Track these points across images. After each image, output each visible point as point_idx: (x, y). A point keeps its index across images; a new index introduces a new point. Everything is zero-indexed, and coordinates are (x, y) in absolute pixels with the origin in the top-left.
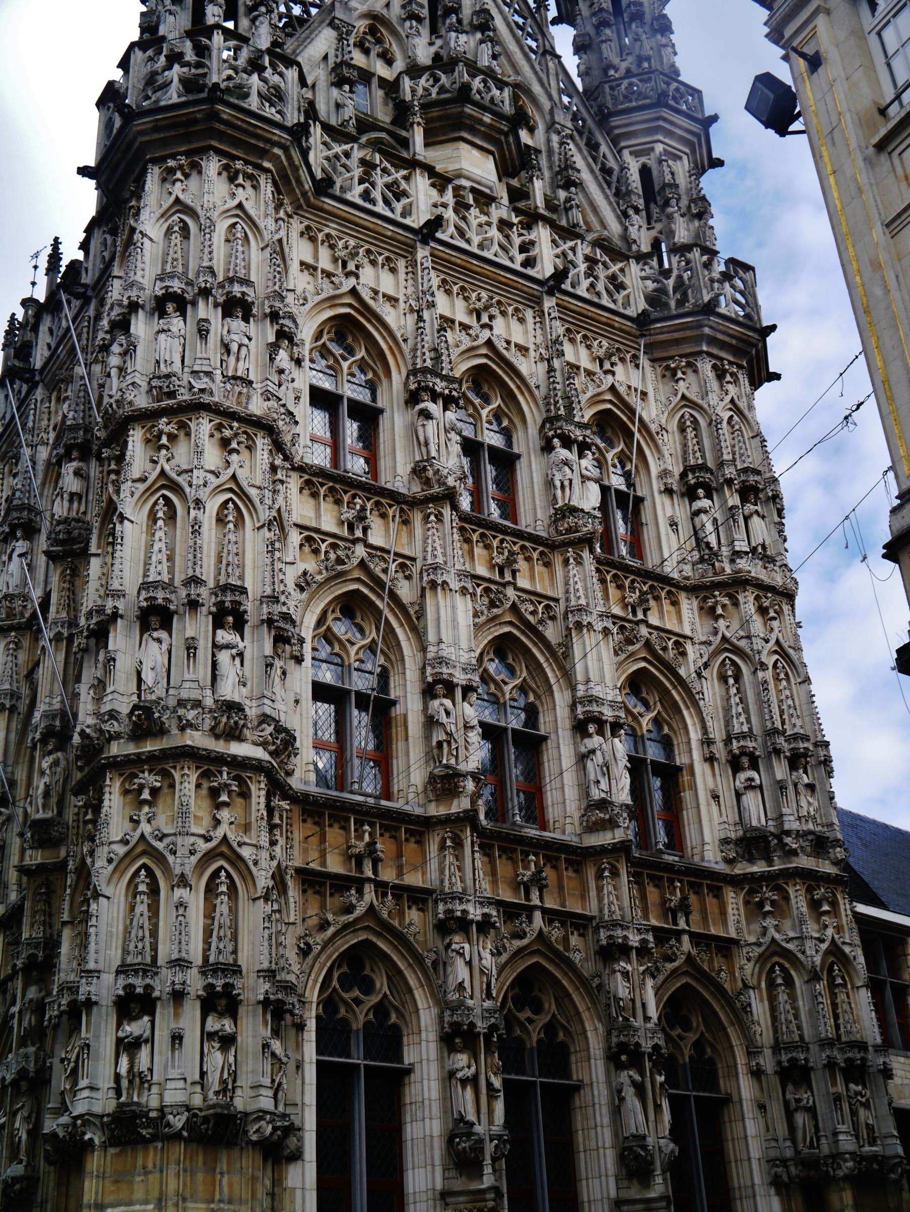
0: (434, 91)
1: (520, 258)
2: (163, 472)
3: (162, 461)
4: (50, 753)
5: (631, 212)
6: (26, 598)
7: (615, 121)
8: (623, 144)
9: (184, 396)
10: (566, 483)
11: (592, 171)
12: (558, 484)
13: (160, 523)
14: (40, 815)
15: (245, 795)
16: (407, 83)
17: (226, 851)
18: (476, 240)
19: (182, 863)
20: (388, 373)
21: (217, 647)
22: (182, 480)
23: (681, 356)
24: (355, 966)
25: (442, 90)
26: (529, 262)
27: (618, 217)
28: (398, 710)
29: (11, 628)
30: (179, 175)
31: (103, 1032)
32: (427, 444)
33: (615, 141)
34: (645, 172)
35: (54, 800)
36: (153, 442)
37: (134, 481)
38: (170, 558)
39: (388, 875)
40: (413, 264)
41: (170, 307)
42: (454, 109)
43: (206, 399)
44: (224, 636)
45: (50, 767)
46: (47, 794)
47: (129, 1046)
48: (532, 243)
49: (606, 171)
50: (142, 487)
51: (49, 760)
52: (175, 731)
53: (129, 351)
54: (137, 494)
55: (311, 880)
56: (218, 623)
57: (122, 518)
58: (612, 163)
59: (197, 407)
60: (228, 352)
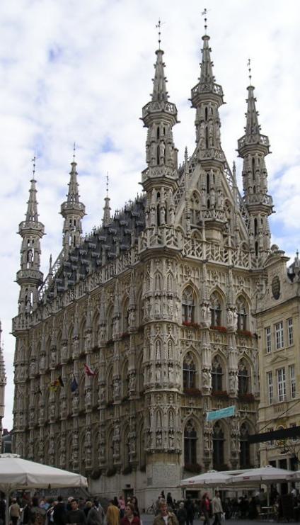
1: (224, 260)
9: (161, 320)
11: (243, 223)
15: (174, 397)
16: (201, 213)
17: (171, 407)
18: (215, 258)
19: (165, 411)
21: (169, 371)
24: (189, 423)
26: (226, 261)
28: (196, 374)
31: (154, 436)
34: (256, 220)
39: (194, 407)
40: (202, 269)
44: (170, 369)
47: (157, 439)
48: (227, 255)
55: (182, 408)
60: (168, 307)
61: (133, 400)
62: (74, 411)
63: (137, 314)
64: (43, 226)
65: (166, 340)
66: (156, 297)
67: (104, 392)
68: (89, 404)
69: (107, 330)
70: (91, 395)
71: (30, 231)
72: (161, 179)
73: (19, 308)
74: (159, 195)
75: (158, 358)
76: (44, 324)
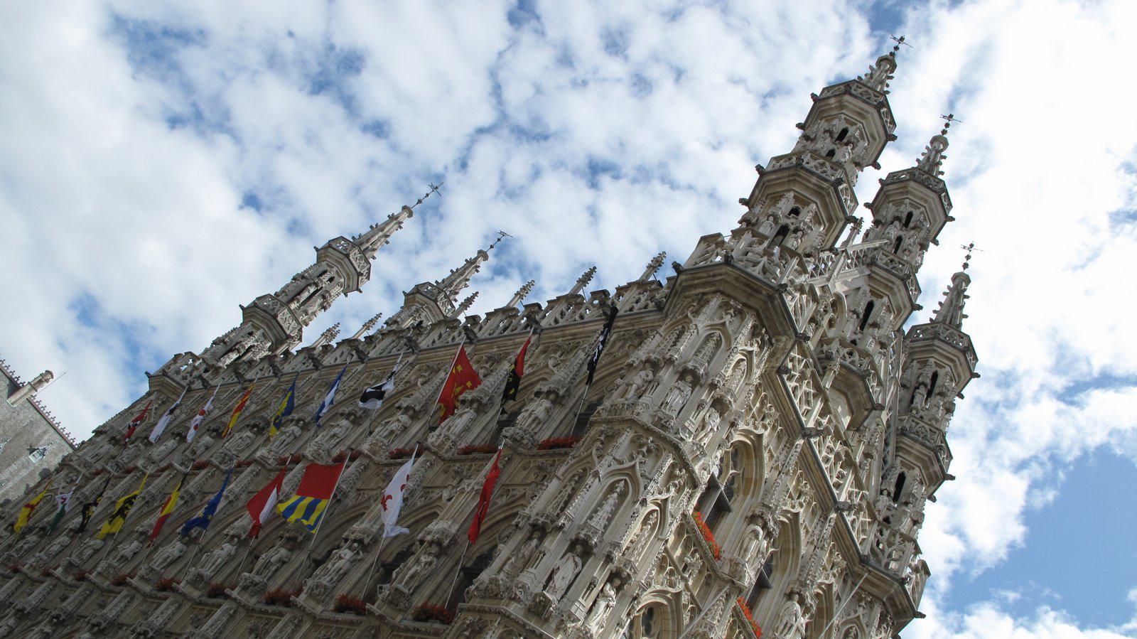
0: (848, 360)
2: (634, 466)
3: (637, 460)
4: (429, 554)
5: (885, 492)
6: (454, 443)
7: (906, 440)
8: (900, 454)
9: (671, 436)
10: (789, 625)
12: (785, 621)
13: (615, 495)
14: (401, 587)
16: (835, 346)
20: (746, 493)
22: (642, 482)
23: (870, 594)
25: (852, 363)
27: (877, 490)
29: (435, 453)
30: (732, 311)
32: (746, 550)
33: (898, 449)
34: (902, 478)
35: (414, 583)
36: (637, 443)
37: (614, 458)
38: (610, 520)
41: (689, 378)
42: (854, 379)
43: (682, 445)
45: (426, 563)
46: (412, 577)
49: (885, 462)
50: (615, 466)
51: (430, 559)
52: (553, 626)
53: (651, 384)
54: (612, 468)
56: (610, 579)
57: (596, 474)
58: (889, 459)
59: (676, 448)
60: (703, 428)
61: (381, 617)
62: (142, 572)
63: (559, 414)
64: (368, 278)
65: (653, 495)
66: (683, 374)
67: (282, 562)
68: (207, 572)
69: (414, 430)
70: (231, 558)
71: (342, 261)
72: (825, 185)
73: (206, 350)
74: (795, 212)
75: (598, 522)
76: (238, 387)
